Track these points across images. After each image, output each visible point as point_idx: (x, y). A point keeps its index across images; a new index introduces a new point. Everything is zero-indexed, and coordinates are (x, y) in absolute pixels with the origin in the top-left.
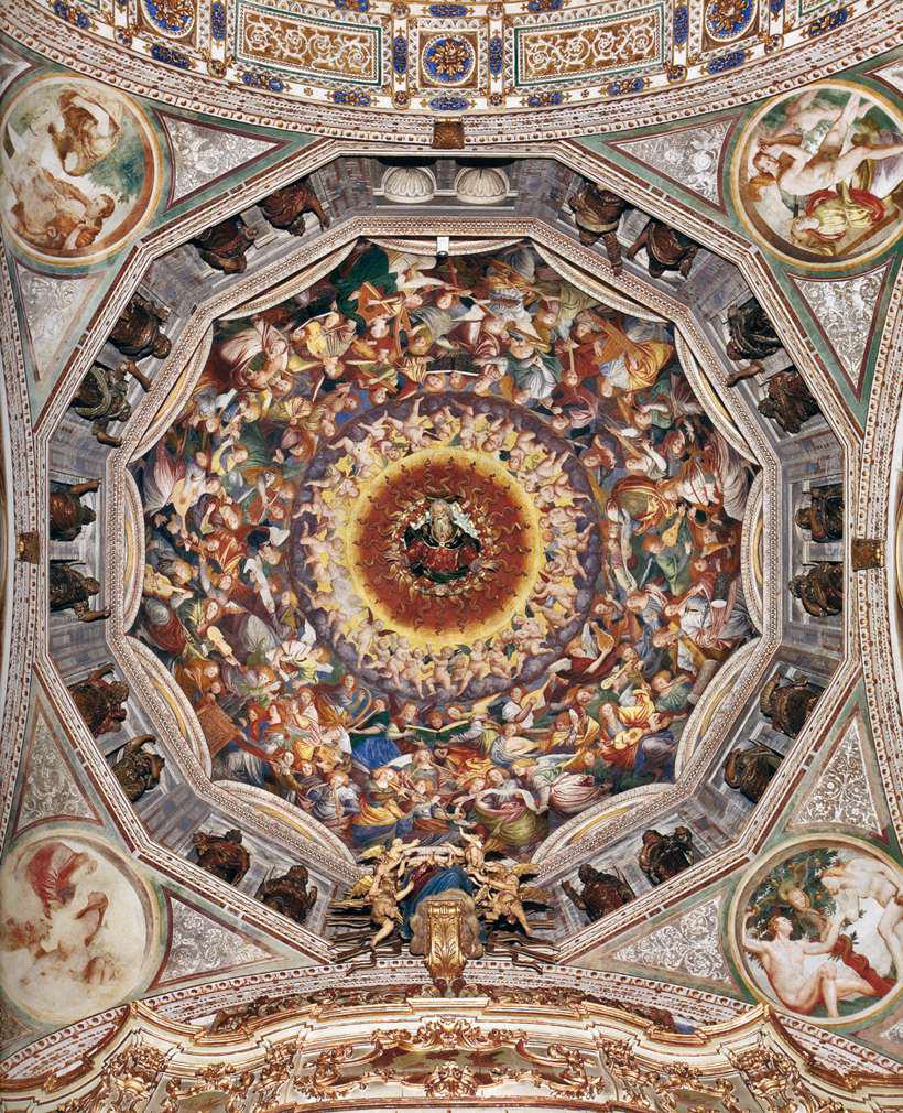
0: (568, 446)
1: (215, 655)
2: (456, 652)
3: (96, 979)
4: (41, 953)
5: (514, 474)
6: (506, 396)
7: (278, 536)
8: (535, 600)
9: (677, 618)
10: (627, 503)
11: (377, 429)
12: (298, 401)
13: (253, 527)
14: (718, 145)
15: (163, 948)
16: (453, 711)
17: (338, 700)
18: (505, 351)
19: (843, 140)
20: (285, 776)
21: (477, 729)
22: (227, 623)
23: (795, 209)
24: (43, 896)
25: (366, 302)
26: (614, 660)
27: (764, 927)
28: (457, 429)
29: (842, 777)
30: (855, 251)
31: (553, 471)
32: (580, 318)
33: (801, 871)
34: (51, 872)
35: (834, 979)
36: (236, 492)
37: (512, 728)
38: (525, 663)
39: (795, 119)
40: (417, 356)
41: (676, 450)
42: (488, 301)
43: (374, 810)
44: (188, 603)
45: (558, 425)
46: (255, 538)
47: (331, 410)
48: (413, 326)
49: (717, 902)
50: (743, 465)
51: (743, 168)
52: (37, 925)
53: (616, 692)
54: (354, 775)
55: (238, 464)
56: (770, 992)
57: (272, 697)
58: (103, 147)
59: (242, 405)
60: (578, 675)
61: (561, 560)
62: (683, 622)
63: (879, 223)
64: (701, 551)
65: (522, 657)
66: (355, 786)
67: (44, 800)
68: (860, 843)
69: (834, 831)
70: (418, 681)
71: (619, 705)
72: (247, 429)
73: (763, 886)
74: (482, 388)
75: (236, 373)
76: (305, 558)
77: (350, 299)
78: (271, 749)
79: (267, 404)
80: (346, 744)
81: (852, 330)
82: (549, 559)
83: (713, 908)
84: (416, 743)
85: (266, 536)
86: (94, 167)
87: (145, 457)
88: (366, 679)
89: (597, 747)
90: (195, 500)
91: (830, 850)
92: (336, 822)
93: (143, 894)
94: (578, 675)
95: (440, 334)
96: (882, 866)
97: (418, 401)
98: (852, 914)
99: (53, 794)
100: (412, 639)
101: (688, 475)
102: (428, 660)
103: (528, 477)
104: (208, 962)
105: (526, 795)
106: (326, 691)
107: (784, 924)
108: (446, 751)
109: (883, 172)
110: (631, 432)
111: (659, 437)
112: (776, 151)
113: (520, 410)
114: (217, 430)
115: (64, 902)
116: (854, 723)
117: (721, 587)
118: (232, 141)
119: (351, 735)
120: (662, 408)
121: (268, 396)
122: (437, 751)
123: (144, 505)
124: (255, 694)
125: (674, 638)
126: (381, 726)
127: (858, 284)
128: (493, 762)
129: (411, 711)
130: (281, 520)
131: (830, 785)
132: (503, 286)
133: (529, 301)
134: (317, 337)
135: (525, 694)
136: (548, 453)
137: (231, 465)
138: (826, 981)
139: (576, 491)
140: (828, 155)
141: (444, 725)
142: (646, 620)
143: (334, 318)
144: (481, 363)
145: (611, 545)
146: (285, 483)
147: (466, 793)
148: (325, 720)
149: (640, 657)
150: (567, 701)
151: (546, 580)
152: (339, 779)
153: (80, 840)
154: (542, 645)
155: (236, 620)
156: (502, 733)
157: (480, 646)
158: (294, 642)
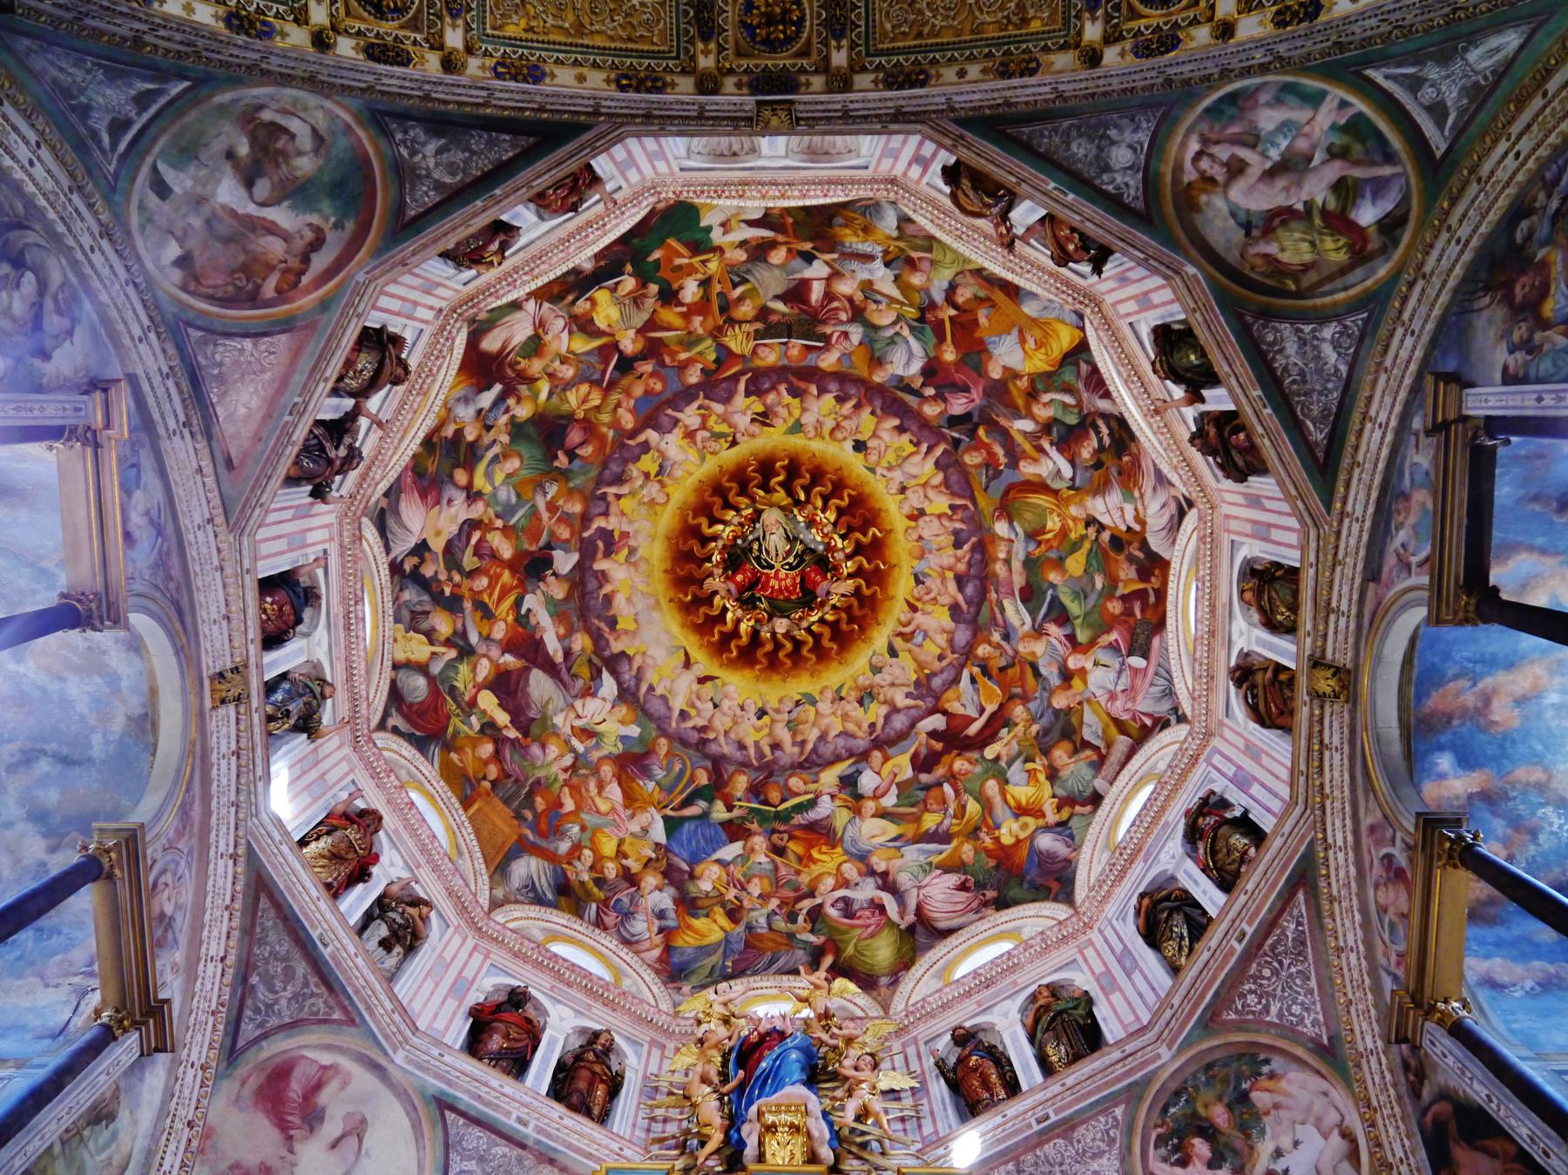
0: (942, 437)
1: (489, 728)
2: (798, 703)
5: (872, 470)
6: (861, 370)
7: (565, 561)
8: (900, 634)
9: (1082, 672)
10: (1020, 516)
11: (690, 416)
12: (584, 388)
13: (531, 553)
14: (1144, 137)
16: (795, 783)
17: (646, 773)
18: (858, 314)
19: (1314, 147)
20: (582, 883)
21: (825, 807)
22: (506, 686)
23: (1247, 227)
24: (283, 1126)
25: (671, 261)
26: (998, 722)
27: (1176, 1149)
28: (797, 413)
29: (1281, 963)
30: (1327, 287)
31: (924, 468)
32: (959, 279)
33: (1226, 1081)
34: (292, 1095)
36: (509, 510)
37: (870, 806)
38: (887, 718)
39: (1250, 115)
40: (740, 323)
41: (1086, 453)
42: (835, 256)
43: (696, 923)
44: (451, 665)
45: (931, 410)
46: (533, 567)
47: (628, 393)
48: (735, 286)
49: (1119, 1112)
50: (1173, 492)
51: (1178, 168)
52: (274, 1162)
53: (1003, 764)
54: (671, 875)
55: (509, 476)
57: (563, 776)
58: (305, 165)
59: (511, 401)
60: (954, 739)
61: (933, 584)
62: (1091, 678)
63: (1360, 255)
64: (1115, 587)
65: (884, 710)
66: (671, 891)
67: (276, 1001)
69: (1268, 1032)
70: (749, 742)
71: (1007, 782)
72: (517, 430)
73: (1177, 1093)
74: (828, 361)
75: (500, 367)
76: (601, 586)
77: (650, 259)
78: (564, 847)
79: (543, 396)
80: (659, 833)
81: (1318, 387)
82: (918, 581)
83: (1115, 1118)
84: (749, 826)
85: (549, 562)
86: (297, 193)
87: (386, 494)
88: (684, 743)
89: (977, 838)
90: (454, 529)
91: (1262, 1057)
92: (647, 945)
93: (410, 1109)
94: (954, 739)
95: (771, 294)
96: (1324, 1085)
97: (743, 380)
98: (1286, 1142)
99: (288, 994)
100: (739, 686)
101: (1101, 489)
102: (762, 713)
103: (889, 475)
105: (888, 900)
106: (632, 763)
107: (1201, 1147)
108: (786, 836)
109: (1368, 194)
110: (1027, 425)
111: (1067, 437)
112: (1223, 152)
113: (880, 390)
114: (479, 437)
115: (312, 1131)
116: (1301, 896)
117: (1141, 639)
118: (478, 141)
119: (666, 819)
120: (1069, 400)
121: (544, 387)
122: (775, 837)
123: (388, 550)
124: (541, 774)
125: (1078, 698)
126: (703, 804)
127: (1328, 332)
128: (846, 852)
129: (741, 783)
130: (567, 541)
131: (1267, 973)
132: (854, 239)
133: (890, 257)
134: (605, 308)
135: (886, 759)
136: (917, 444)
137: (499, 477)
139: (954, 494)
140: (1290, 166)
141: (783, 800)
142: (1043, 671)
143: (629, 283)
144: (828, 330)
145: (999, 568)
146: (571, 493)
147: (812, 894)
148: (630, 799)
149: (1033, 720)
150: (940, 771)
151: (914, 609)
152: (651, 880)
153: (329, 1048)
154: (908, 695)
155: (514, 678)
156: (857, 812)
157: (829, 695)
158: (589, 700)
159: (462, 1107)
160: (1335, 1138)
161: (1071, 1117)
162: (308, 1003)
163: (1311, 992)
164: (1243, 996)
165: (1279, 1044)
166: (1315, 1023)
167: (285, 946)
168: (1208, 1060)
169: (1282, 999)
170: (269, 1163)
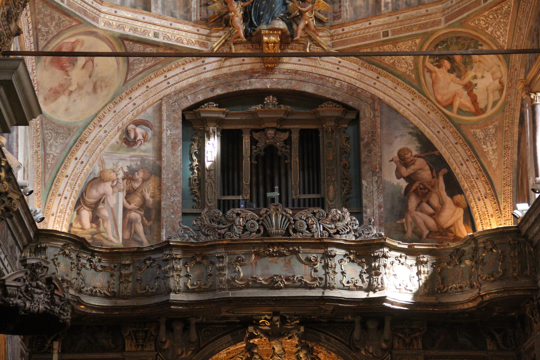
3: (99, 90)
4: (71, 92)
15: (126, 64)
29: (498, 16)
35: (460, 98)
49: (418, 41)
56: (431, 90)
67: (50, 29)
69: (485, 36)
73: (443, 42)
83: (416, 43)
91: (480, 43)
96: (500, 63)
98: (479, 75)
104: (148, 63)
107: (447, 64)
115: (74, 65)
138: (456, 97)
159: (131, 38)
160: (497, 82)
161: (398, 38)
162: (62, 25)
164: (479, 20)
165: (488, 41)
166: (503, 41)
168: (459, 35)
169: (494, 27)
170: (62, 83)
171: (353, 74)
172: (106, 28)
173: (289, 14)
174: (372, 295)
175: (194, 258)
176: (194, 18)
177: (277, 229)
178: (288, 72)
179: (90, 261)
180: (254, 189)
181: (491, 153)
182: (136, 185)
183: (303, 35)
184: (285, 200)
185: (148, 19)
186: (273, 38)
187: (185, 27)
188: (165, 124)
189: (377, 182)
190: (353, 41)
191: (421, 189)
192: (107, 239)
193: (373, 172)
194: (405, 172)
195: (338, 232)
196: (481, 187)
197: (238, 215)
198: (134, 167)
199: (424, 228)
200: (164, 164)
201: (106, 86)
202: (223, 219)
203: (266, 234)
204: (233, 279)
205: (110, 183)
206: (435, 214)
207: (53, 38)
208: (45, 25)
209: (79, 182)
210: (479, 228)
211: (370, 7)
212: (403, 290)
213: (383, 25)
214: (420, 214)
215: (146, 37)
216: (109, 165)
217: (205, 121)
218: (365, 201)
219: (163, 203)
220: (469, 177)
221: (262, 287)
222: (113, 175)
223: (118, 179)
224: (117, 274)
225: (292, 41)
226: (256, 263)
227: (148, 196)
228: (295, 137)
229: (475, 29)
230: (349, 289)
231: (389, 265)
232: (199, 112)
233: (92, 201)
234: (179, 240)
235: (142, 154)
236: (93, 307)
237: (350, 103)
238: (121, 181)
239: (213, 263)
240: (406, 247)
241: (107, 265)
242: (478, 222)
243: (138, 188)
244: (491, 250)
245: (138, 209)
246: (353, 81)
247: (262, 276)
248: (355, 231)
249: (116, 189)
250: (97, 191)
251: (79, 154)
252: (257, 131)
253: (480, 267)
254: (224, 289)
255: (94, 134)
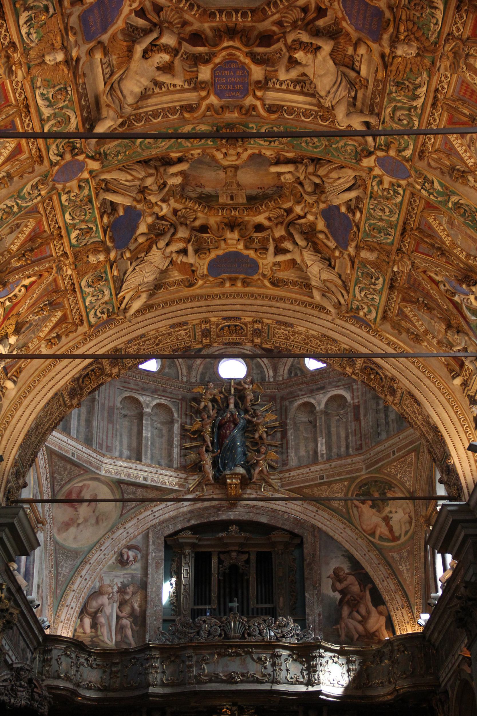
3: (100, 523)
4: (79, 524)
49: (346, 483)
56: (358, 521)
68: (404, 490)
73: (365, 485)
98: (394, 510)
116: (413, 454)
153: (81, 481)
160: (407, 516)
163: (410, 476)
165: (398, 485)
166: (410, 485)
167: (63, 463)
171: (297, 508)
172: (106, 475)
173: (248, 462)
174: (311, 689)
175: (169, 658)
176: (175, 466)
177: (235, 633)
178: (247, 506)
179: (87, 660)
180: (222, 599)
181: (405, 572)
182: (127, 597)
183: (259, 478)
184: (243, 611)
185: (139, 467)
186: (234, 481)
187: (168, 473)
188: (151, 548)
189: (317, 594)
190: (298, 483)
191: (352, 600)
192: (103, 641)
193: (314, 586)
194: (339, 586)
195: (283, 636)
196: (399, 598)
197: (204, 622)
198: (126, 582)
199: (355, 633)
200: (150, 580)
201: (106, 519)
202: (192, 625)
203: (227, 637)
204: (200, 675)
205: (107, 596)
206: (364, 621)
207: (66, 483)
208: (60, 474)
209: (83, 595)
210: (398, 633)
211: (311, 456)
212: (336, 685)
213: (319, 471)
214: (350, 620)
215: (137, 481)
216: (107, 581)
217: (182, 546)
218: (307, 610)
219: (148, 612)
220: (389, 591)
221: (222, 681)
222: (109, 590)
223: (113, 592)
224: (108, 671)
225: (250, 483)
226: (218, 662)
227: (136, 606)
228: (253, 557)
229: (389, 475)
230: (292, 683)
231: (324, 663)
232: (177, 539)
233: (93, 610)
234: (157, 642)
235: (133, 572)
236: (88, 699)
237: (296, 531)
238: (115, 594)
239: (184, 662)
240: (338, 648)
241: (100, 663)
242: (397, 628)
243: (128, 600)
244: (403, 652)
245: (128, 617)
246: (298, 513)
247: (222, 672)
248: (298, 635)
249: (111, 601)
250: (97, 602)
251: (83, 573)
252: (224, 553)
253: (396, 666)
254: (192, 684)
255: (96, 556)
